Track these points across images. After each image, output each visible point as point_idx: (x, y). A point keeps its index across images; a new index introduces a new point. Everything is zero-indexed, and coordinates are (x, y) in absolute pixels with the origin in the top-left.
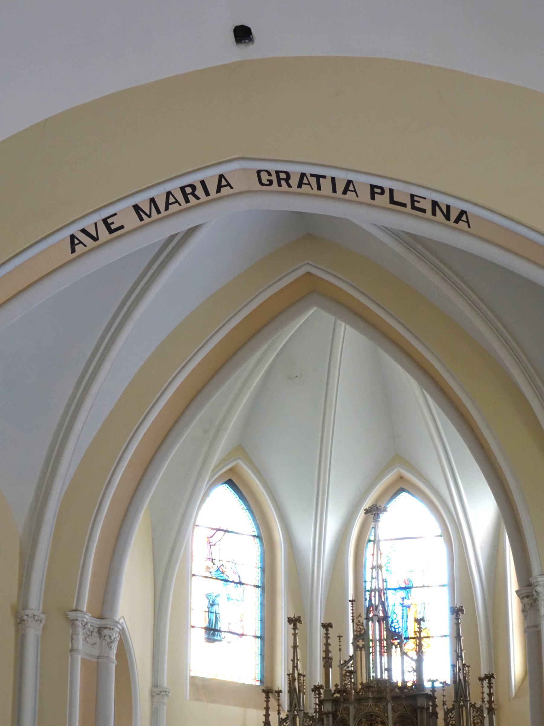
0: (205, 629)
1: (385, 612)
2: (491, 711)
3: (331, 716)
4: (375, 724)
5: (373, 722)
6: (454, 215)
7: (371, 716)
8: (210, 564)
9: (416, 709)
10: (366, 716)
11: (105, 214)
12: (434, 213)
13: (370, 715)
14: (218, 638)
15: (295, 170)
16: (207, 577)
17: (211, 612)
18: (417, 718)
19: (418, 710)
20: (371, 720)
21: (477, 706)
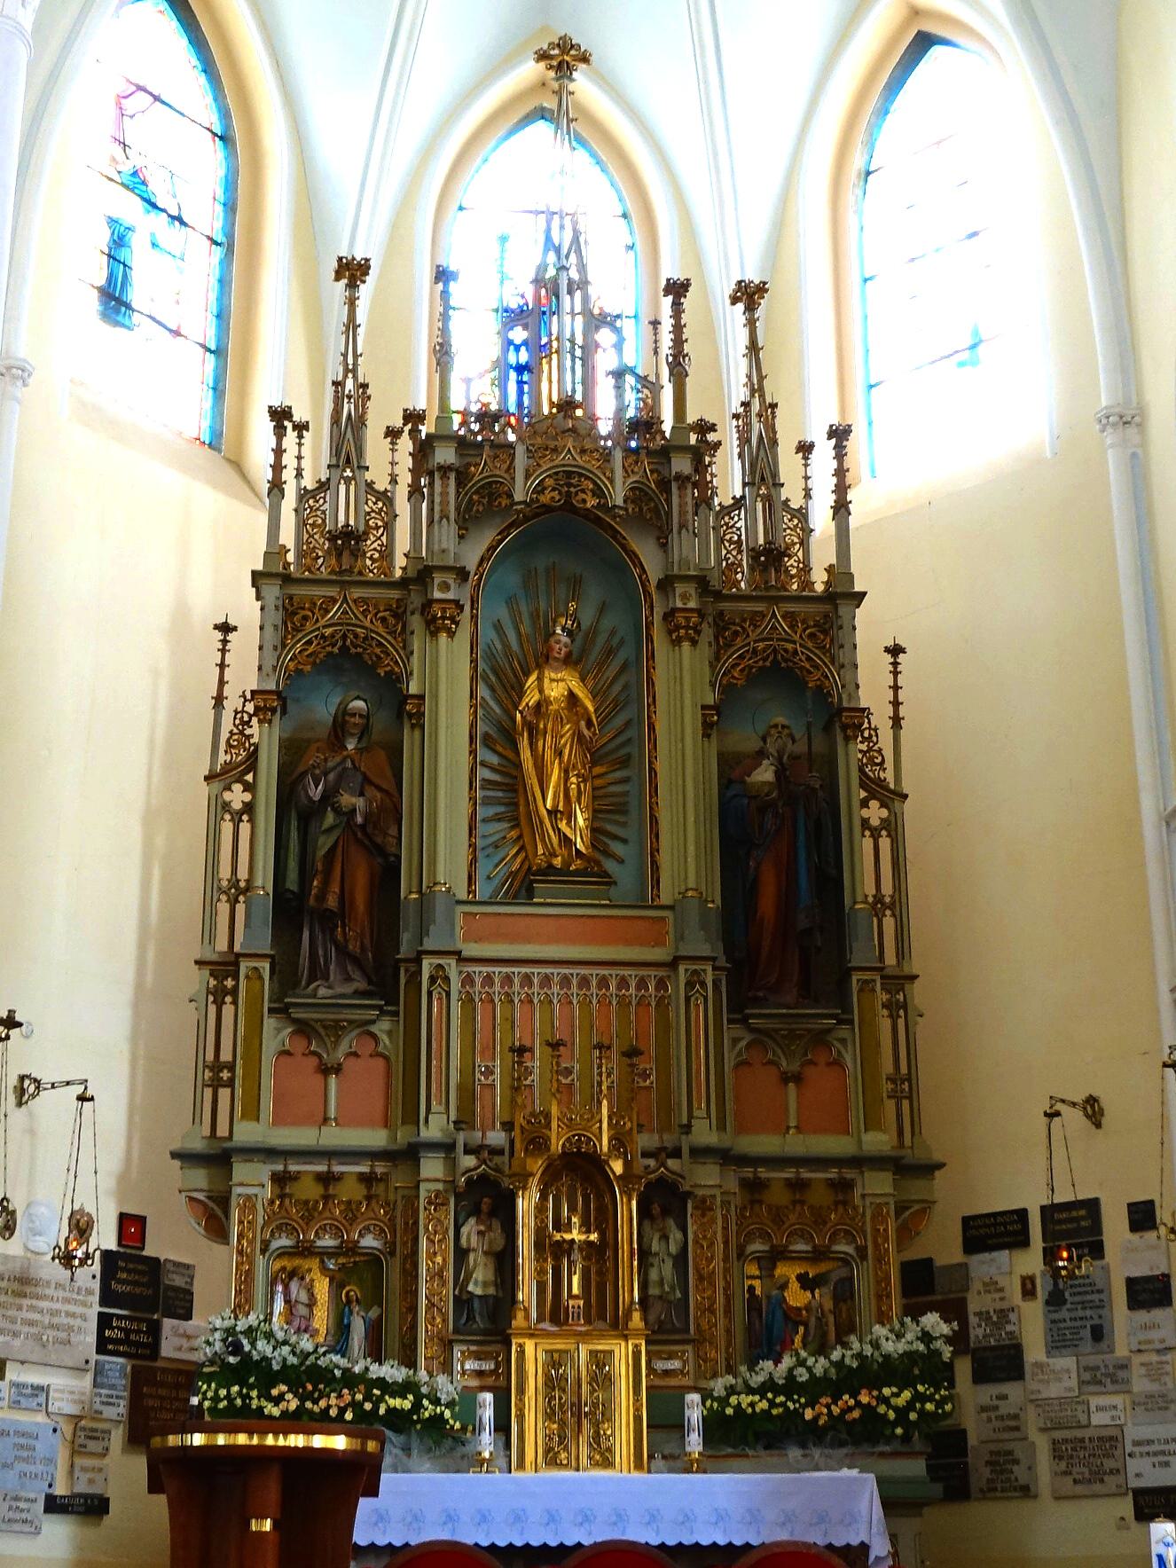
0: (99, 292)
1: (582, 268)
3: (452, 476)
4: (576, 494)
5: (572, 489)
7: (569, 474)
8: (117, 151)
9: (670, 482)
10: (556, 473)
13: (564, 471)
14: (127, 322)
17: (115, 259)
19: (674, 486)
20: (569, 485)
21: (794, 505)
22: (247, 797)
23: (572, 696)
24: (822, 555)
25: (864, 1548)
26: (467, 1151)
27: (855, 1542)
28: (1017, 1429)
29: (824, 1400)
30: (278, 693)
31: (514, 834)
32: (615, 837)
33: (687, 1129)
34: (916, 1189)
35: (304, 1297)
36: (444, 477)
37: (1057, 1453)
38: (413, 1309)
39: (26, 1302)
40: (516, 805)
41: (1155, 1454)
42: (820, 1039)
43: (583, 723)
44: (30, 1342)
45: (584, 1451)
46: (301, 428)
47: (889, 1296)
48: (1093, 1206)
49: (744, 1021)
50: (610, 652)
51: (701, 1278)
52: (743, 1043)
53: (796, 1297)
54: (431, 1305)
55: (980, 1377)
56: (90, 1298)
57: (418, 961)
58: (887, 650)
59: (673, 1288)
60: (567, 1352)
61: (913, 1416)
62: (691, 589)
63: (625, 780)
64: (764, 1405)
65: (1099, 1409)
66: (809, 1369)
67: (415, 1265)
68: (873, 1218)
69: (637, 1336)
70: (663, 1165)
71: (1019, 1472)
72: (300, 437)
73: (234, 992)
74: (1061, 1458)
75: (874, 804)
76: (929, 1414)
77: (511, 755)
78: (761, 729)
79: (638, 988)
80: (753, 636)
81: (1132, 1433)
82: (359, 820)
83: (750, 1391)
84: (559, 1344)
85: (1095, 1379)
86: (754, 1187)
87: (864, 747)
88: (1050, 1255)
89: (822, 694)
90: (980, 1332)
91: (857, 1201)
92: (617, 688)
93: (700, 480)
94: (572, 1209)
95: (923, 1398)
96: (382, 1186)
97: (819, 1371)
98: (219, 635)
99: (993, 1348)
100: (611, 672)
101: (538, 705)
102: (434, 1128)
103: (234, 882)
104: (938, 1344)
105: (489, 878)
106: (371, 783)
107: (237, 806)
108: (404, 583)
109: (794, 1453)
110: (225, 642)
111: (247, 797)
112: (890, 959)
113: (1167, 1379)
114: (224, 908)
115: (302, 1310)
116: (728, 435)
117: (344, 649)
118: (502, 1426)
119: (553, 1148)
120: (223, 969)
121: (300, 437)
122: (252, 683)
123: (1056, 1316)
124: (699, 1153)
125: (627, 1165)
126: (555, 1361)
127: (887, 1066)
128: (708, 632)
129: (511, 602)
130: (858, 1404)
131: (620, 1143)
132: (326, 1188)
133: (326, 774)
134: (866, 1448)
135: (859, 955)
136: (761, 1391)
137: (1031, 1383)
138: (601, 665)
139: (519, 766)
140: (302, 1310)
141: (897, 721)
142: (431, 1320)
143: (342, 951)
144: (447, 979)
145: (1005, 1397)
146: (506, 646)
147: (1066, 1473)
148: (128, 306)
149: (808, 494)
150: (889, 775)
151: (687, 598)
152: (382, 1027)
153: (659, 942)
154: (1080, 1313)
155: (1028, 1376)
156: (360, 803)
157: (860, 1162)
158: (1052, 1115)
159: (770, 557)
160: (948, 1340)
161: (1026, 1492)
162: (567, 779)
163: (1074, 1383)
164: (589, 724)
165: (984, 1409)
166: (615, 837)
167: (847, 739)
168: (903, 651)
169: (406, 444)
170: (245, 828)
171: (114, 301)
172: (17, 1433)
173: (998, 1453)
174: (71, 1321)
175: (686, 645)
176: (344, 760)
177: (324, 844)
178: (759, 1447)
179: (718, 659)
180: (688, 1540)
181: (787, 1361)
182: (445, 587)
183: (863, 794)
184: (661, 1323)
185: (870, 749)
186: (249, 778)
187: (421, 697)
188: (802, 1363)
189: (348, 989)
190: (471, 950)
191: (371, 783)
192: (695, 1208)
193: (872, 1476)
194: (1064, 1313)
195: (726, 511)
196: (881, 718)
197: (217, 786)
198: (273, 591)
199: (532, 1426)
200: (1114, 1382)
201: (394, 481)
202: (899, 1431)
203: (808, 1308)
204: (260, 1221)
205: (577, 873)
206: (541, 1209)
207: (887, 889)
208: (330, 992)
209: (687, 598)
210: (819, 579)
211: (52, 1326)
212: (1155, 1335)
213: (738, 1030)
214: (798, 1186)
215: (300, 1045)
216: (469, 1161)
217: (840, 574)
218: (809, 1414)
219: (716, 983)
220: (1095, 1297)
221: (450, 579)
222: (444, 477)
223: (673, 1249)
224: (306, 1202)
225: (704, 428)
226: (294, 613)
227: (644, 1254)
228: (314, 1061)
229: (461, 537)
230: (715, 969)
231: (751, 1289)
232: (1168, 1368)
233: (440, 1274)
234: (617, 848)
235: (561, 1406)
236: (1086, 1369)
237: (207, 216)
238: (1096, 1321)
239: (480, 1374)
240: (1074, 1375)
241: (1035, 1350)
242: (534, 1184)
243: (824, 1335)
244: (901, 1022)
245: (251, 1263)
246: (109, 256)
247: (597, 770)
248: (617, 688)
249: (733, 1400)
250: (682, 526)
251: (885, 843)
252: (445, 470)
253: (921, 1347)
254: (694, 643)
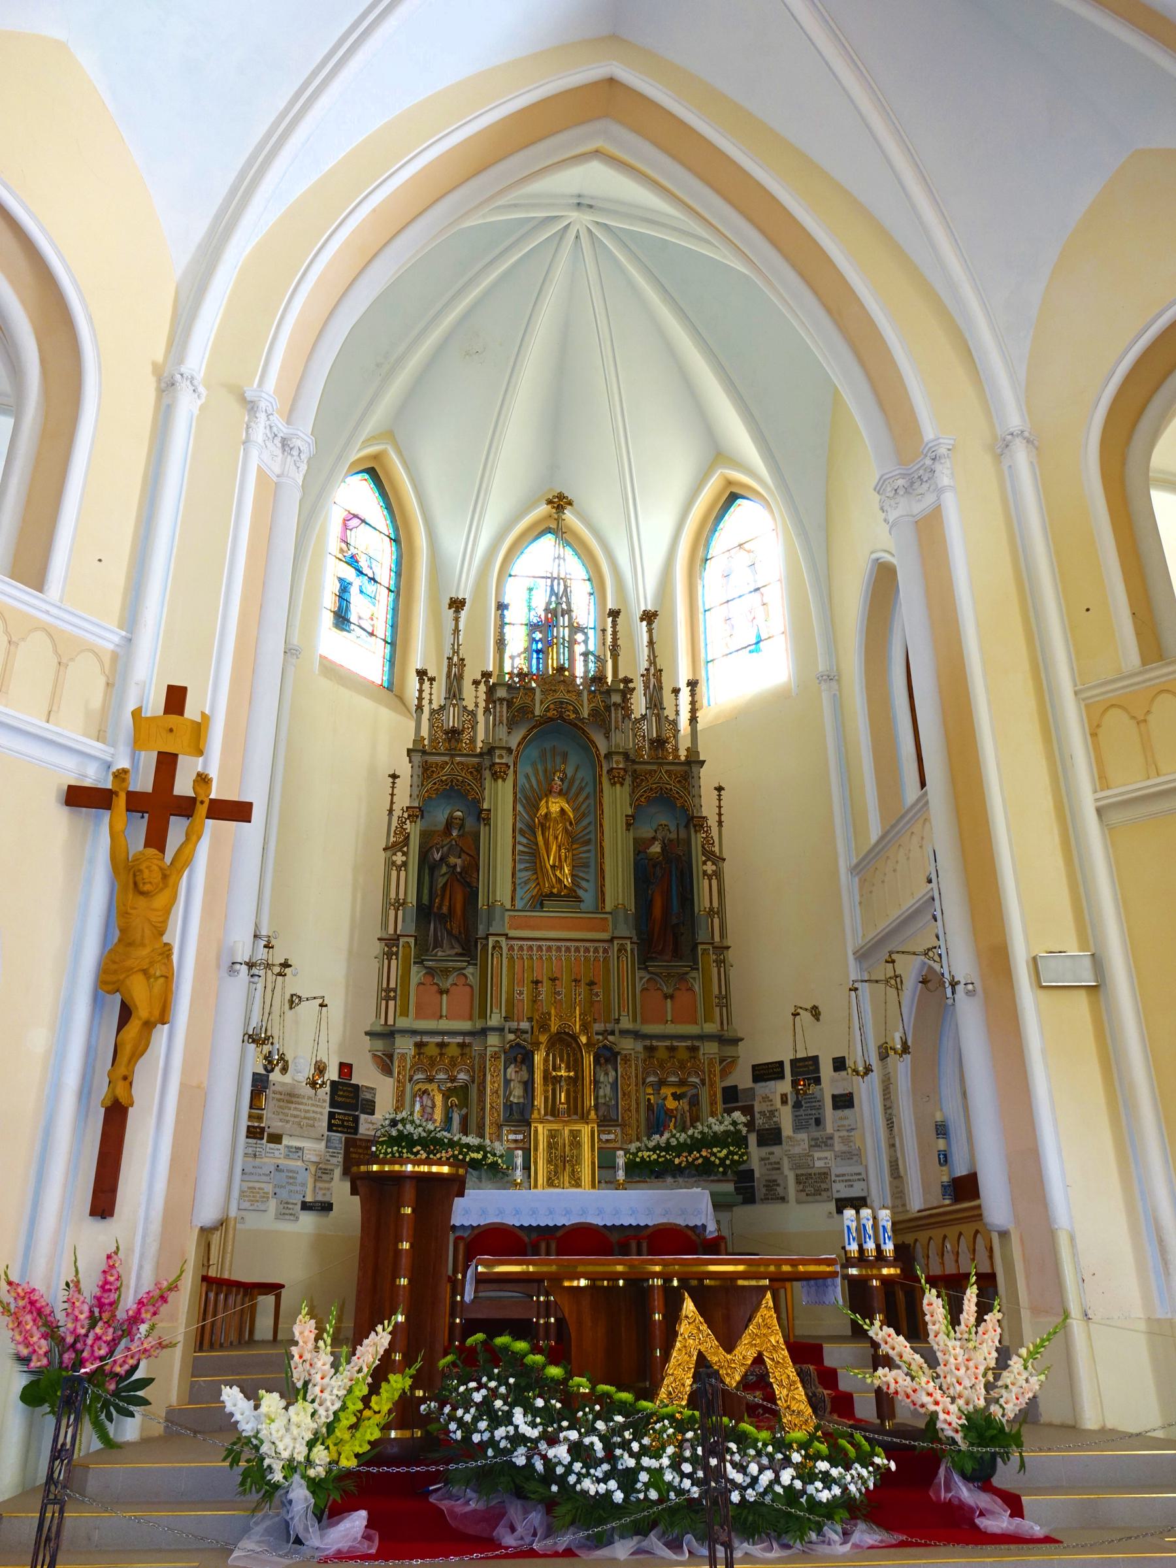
1: (568, 603)
3: (505, 703)
7: (562, 703)
8: (344, 546)
16: (340, 560)
18: (610, 716)
19: (613, 709)
20: (562, 708)
21: (671, 718)
22: (404, 858)
23: (562, 810)
24: (684, 743)
25: (704, 1227)
26: (510, 1032)
27: (699, 1224)
28: (779, 1169)
29: (685, 1154)
30: (419, 808)
31: (534, 877)
32: (583, 879)
33: (618, 1021)
34: (729, 1051)
35: (429, 1103)
36: (501, 704)
37: (798, 1182)
38: (483, 1109)
39: (293, 1106)
40: (536, 863)
41: (846, 1181)
42: (682, 977)
43: (568, 824)
44: (295, 1126)
45: (567, 1178)
46: (432, 680)
47: (716, 1103)
48: (815, 1059)
49: (646, 968)
50: (581, 789)
51: (624, 1094)
52: (645, 980)
53: (671, 1104)
54: (492, 1108)
55: (761, 1143)
56: (324, 1104)
57: (487, 938)
58: (716, 789)
59: (610, 1099)
60: (558, 1130)
61: (728, 1162)
62: (620, 758)
63: (589, 851)
64: (655, 1157)
65: (819, 1159)
66: (677, 1139)
67: (485, 1088)
68: (709, 1064)
69: (593, 1123)
70: (606, 1039)
71: (780, 1190)
72: (431, 684)
73: (397, 954)
74: (800, 1183)
75: (709, 863)
76: (736, 1161)
77: (532, 838)
78: (655, 826)
79: (594, 953)
80: (651, 782)
81: (835, 1171)
82: (459, 870)
83: (648, 1150)
84: (555, 1126)
85: (816, 1144)
86: (650, 1050)
87: (704, 835)
88: (795, 1083)
89: (685, 810)
90: (761, 1121)
91: (701, 1057)
92: (584, 807)
93: (625, 707)
94: (561, 1060)
95: (733, 1153)
96: (468, 1049)
97: (682, 1140)
98: (391, 780)
99: (767, 1129)
100: (581, 799)
101: (546, 815)
102: (495, 1020)
103: (397, 900)
104: (740, 1127)
105: (522, 899)
106: (464, 852)
107: (399, 863)
108: (481, 755)
109: (670, 1180)
110: (394, 783)
111: (404, 858)
112: (717, 938)
113: (851, 1144)
114: (392, 913)
115: (429, 1110)
116: (639, 684)
117: (452, 787)
118: (526, 1168)
119: (552, 1030)
120: (391, 943)
121: (431, 684)
122: (407, 803)
123: (798, 1113)
124: (624, 1033)
125: (589, 1038)
126: (552, 1135)
127: (716, 991)
128: (628, 780)
129: (534, 764)
130: (701, 1156)
131: (585, 1027)
132: (441, 1050)
133: (442, 847)
134: (704, 1177)
135: (702, 936)
136: (654, 1150)
137: (785, 1146)
138: (577, 795)
139: (537, 844)
140: (429, 1110)
141: (720, 823)
142: (492, 1115)
143: (450, 933)
144: (501, 948)
145: (772, 1153)
146: (531, 786)
147: (802, 1191)
148: (348, 621)
149: (677, 713)
150: (716, 849)
151: (618, 763)
152: (470, 970)
153: (604, 931)
154: (810, 1112)
155: (784, 1143)
156: (459, 861)
157: (702, 1037)
158: (795, 1015)
159: (659, 743)
160: (745, 1125)
161: (783, 1199)
162: (560, 850)
163: (806, 1146)
164: (571, 824)
165: (762, 1159)
166: (583, 879)
167: (696, 832)
168: (723, 789)
169: (482, 688)
170: (403, 873)
171: (342, 619)
172: (288, 1171)
173: (770, 1181)
174: (316, 1116)
175: (618, 786)
176: (451, 841)
177: (441, 881)
178: (653, 1177)
179: (633, 792)
180: (617, 1223)
181: (666, 1135)
182: (501, 757)
183: (704, 858)
184: (604, 1116)
185: (707, 837)
186: (405, 849)
187: (489, 810)
188: (673, 1136)
189: (453, 952)
190: (512, 933)
191: (464, 852)
192: (622, 1060)
193: (707, 1192)
194: (801, 1112)
195: (637, 721)
196: (712, 821)
197: (389, 853)
198: (417, 758)
199: (541, 1168)
200: (826, 1145)
201: (477, 706)
202: (721, 1169)
203: (676, 1109)
204: (409, 1067)
205: (565, 896)
206: (546, 1060)
207: (715, 904)
208: (443, 954)
209: (618, 763)
210: (683, 754)
211: (305, 1118)
212: (846, 1122)
213: (643, 973)
214: (672, 1049)
215: (429, 980)
216: (511, 1037)
217: (693, 751)
218: (677, 1161)
219: (632, 950)
220: (817, 1104)
221: (504, 752)
222: (501, 704)
223: (611, 1080)
224: (431, 1057)
225: (627, 681)
226: (428, 769)
227: (596, 1083)
228: (435, 987)
229: (509, 733)
230: (631, 943)
231: (649, 1100)
232: (852, 1139)
233: (496, 1092)
234: (584, 884)
235: (556, 1157)
236: (812, 1139)
237: (385, 576)
238: (818, 1116)
239: (516, 1141)
240: (806, 1142)
241: (787, 1129)
242: (543, 1047)
243: (685, 1122)
244: (722, 969)
245: (404, 1087)
246: (339, 596)
247: (575, 846)
248: (584, 807)
249: (640, 1154)
250: (616, 728)
251: (714, 882)
252: (501, 700)
253: (732, 1128)
254: (622, 785)
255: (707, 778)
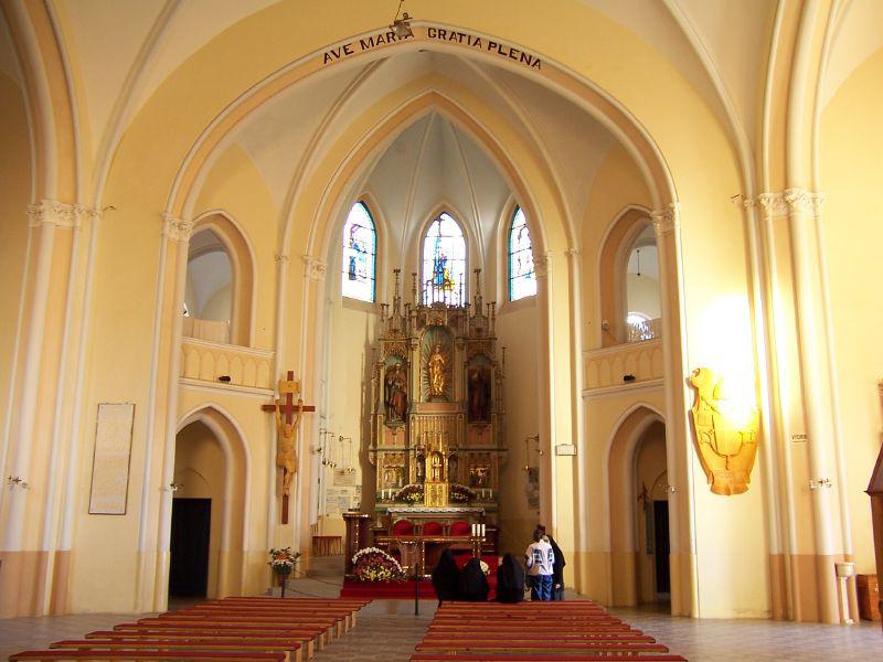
2: (493, 319)
6: (533, 62)
11: (345, 43)
12: (521, 60)
15: (450, 29)
53: (480, 474)
102: (412, 446)
131: (444, 448)
171: (352, 275)
209: (461, 341)
237: (371, 249)
255: (498, 345)
